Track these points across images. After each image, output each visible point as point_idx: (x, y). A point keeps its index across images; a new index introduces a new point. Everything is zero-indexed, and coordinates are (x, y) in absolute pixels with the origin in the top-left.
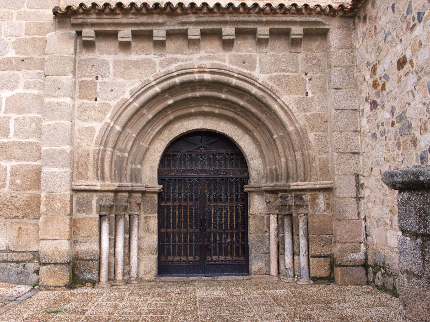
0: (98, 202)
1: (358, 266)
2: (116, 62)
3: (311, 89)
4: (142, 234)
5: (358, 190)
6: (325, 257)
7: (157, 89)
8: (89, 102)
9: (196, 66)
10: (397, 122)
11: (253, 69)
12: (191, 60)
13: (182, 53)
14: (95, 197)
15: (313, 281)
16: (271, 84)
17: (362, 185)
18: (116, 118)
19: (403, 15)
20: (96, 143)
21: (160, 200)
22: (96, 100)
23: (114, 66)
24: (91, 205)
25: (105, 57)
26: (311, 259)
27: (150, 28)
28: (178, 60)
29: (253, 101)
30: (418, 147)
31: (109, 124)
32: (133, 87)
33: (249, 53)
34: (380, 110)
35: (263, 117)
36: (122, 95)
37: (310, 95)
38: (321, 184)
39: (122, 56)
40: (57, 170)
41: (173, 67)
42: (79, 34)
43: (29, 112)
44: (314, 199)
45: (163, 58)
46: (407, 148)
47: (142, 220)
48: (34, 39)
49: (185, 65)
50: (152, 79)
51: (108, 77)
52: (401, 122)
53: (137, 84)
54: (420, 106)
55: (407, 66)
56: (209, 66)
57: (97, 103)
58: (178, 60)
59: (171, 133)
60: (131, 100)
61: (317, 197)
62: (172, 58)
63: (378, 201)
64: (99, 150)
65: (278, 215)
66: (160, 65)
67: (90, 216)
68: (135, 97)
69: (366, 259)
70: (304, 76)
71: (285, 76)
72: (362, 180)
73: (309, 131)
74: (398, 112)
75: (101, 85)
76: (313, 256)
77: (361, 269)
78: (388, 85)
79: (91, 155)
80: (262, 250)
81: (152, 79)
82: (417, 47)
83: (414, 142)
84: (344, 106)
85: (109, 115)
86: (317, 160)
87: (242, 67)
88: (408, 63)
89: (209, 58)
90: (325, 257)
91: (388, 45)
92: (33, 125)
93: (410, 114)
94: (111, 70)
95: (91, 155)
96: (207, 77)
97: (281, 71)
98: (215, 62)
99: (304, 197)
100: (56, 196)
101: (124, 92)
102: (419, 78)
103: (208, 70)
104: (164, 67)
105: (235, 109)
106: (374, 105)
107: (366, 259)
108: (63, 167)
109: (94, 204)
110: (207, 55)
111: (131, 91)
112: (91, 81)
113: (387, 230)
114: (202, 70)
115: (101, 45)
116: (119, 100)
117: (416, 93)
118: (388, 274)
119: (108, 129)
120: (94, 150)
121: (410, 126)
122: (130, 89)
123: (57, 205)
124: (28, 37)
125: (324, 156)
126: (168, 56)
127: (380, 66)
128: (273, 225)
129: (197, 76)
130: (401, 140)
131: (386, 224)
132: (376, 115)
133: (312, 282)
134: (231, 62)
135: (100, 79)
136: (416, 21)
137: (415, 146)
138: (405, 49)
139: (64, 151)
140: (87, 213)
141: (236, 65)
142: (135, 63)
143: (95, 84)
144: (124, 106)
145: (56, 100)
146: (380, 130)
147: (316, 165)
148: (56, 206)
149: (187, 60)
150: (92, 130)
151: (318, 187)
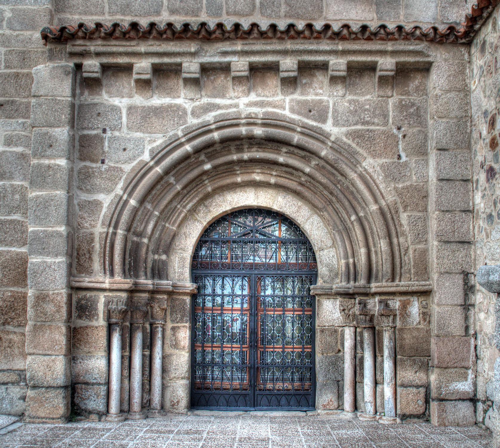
1: (463, 400)
3: (404, 150)
5: (466, 295)
6: (418, 387)
9: (243, 116)
11: (324, 120)
12: (236, 106)
13: (223, 96)
15: (402, 420)
16: (349, 142)
18: (130, 188)
20: (103, 224)
22: (103, 162)
23: (128, 115)
25: (116, 101)
26: (399, 389)
27: (178, 60)
28: (218, 107)
31: (121, 198)
32: (155, 145)
33: (318, 98)
36: (139, 156)
37: (404, 159)
38: (416, 285)
41: (210, 117)
43: (11, 178)
44: (405, 306)
45: (197, 103)
48: (17, 75)
49: (228, 114)
50: (180, 134)
53: (160, 141)
57: (105, 166)
60: (152, 163)
62: (209, 104)
66: (193, 113)
68: (156, 159)
70: (395, 131)
71: (368, 130)
73: (401, 210)
75: (109, 141)
76: (402, 385)
77: (468, 404)
81: (180, 134)
85: (121, 185)
86: (411, 252)
87: (308, 118)
89: (261, 104)
90: (418, 387)
92: (17, 197)
94: (124, 119)
95: (97, 239)
96: (258, 131)
97: (363, 124)
98: (270, 109)
99: (390, 303)
101: (143, 152)
104: (198, 117)
107: (475, 390)
111: (152, 151)
112: (96, 136)
114: (252, 120)
116: (135, 163)
120: (101, 233)
122: (150, 148)
124: (8, 71)
129: (243, 130)
134: (292, 110)
135: (109, 134)
139: (59, 234)
141: (299, 114)
142: (158, 111)
143: (102, 140)
149: (231, 106)
151: (410, 289)
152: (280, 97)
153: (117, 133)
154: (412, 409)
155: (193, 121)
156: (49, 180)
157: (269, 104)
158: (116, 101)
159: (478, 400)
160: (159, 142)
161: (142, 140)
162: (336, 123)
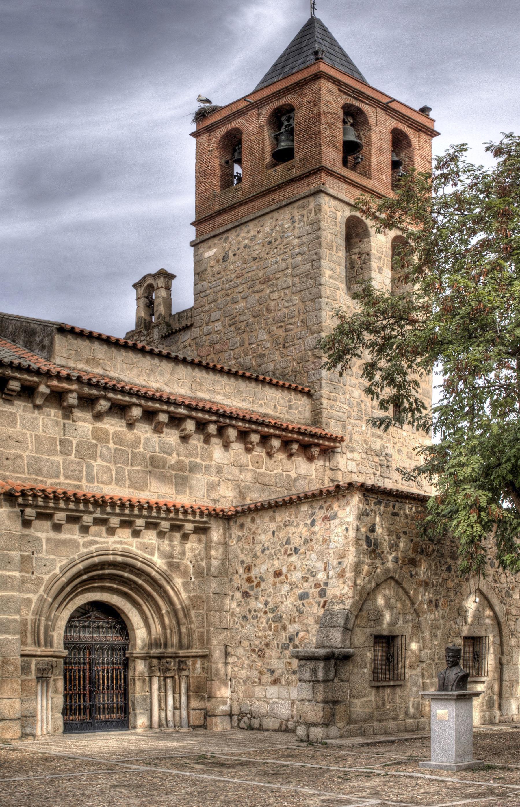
0: (36, 666)
1: (226, 715)
2: (48, 540)
3: (193, 575)
4: (53, 695)
5: (226, 657)
7: (81, 566)
8: (27, 575)
9: (111, 549)
10: (270, 612)
11: (153, 554)
12: (107, 543)
14: (34, 661)
15: (193, 729)
17: (229, 653)
18: (47, 590)
19: (282, 543)
20: (33, 613)
21: (65, 663)
22: (33, 573)
23: (47, 543)
24: (30, 668)
25: (39, 534)
28: (96, 542)
29: (148, 581)
30: (287, 631)
32: (62, 563)
33: (150, 541)
34: (253, 600)
35: (155, 594)
36: (53, 570)
37: (193, 579)
38: (200, 652)
39: (52, 535)
40: (10, 637)
41: (93, 548)
42: (22, 511)
44: (194, 663)
45: (86, 539)
46: (277, 631)
47: (52, 683)
49: (103, 547)
50: (76, 557)
51: (41, 553)
52: (273, 612)
54: (291, 606)
55: (282, 578)
56: (121, 550)
57: (34, 576)
58: (96, 542)
59: (75, 603)
60: (61, 575)
61: (196, 663)
62: (92, 540)
63: (245, 666)
64: (36, 619)
65: (159, 677)
66: (83, 545)
67: (29, 677)
68: (63, 572)
69: (231, 710)
72: (229, 650)
73: (191, 609)
74: (271, 605)
75: (36, 560)
76: (193, 709)
77: (228, 718)
78: (263, 585)
79: (29, 623)
80: (145, 707)
81: (76, 557)
82: (292, 568)
83: (284, 628)
84: (219, 591)
85: (42, 588)
86: (196, 632)
87: (145, 552)
88: (284, 575)
89: (121, 543)
90: (201, 709)
91: (266, 557)
93: (282, 608)
94: (44, 547)
95: (29, 623)
96: (119, 559)
99: (187, 662)
100: (9, 660)
101: (55, 568)
102: (292, 589)
103: (120, 553)
104: (86, 548)
105: (130, 585)
106: (246, 594)
107: (231, 710)
108: (15, 634)
109: (33, 666)
110: (119, 539)
111: (60, 568)
112: (28, 556)
113: (255, 686)
114: (116, 552)
115: (37, 523)
117: (288, 597)
118: (254, 718)
119: (41, 600)
120: (32, 619)
121: (281, 617)
123: (11, 668)
125: (201, 630)
126: (90, 538)
127: (257, 568)
128: (155, 686)
129: (111, 558)
130: (273, 625)
131: (254, 682)
132: (248, 604)
133: (192, 730)
134: (137, 548)
135: (35, 555)
136: (293, 552)
137: (285, 631)
138: (282, 566)
139: (15, 620)
140: (27, 675)
141: (141, 550)
142: (64, 543)
143: (32, 559)
144: (55, 580)
145: (8, 573)
146: (252, 614)
147: (195, 636)
148: (10, 669)
150: (29, 601)
151: (198, 654)
152: (131, 539)
153: (40, 555)
154: (197, 723)
155: (83, 550)
156: (9, 585)
157: (125, 543)
158: (39, 534)
159: (233, 715)
160: (64, 562)
161: (54, 560)
162: (160, 557)
